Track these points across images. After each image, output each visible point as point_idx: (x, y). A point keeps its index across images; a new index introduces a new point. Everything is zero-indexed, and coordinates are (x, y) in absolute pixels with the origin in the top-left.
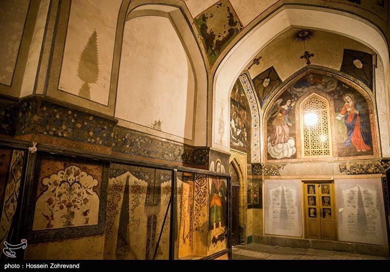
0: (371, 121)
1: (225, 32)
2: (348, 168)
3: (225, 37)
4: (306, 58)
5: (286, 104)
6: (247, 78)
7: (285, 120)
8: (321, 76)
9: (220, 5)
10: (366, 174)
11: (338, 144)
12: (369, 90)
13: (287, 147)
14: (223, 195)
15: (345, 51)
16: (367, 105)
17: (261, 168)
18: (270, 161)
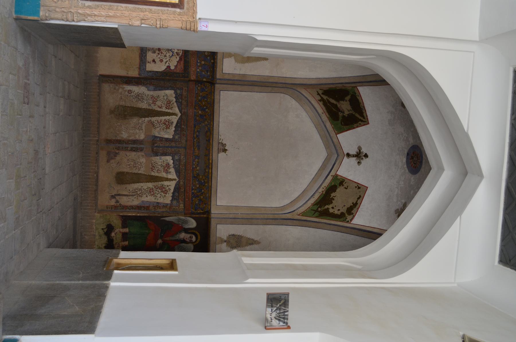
1: (339, 210)
9: (359, 188)
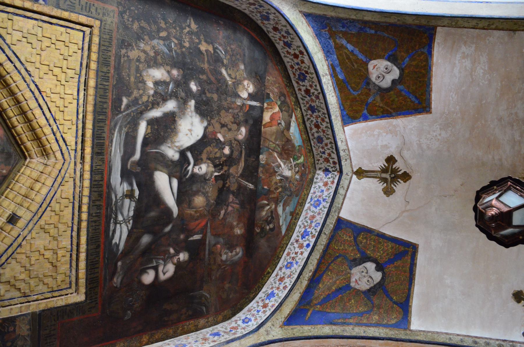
6: (332, 191)
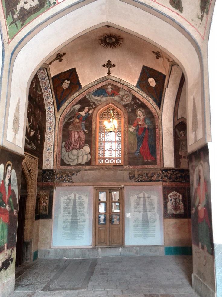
0: (157, 135)
2: (136, 176)
3: (33, 7)
4: (108, 67)
5: (84, 110)
7: (82, 126)
8: (119, 88)
10: (150, 181)
11: (129, 153)
12: (157, 108)
13: (82, 153)
14: (11, 208)
15: (143, 69)
16: (155, 121)
17: (54, 174)
18: (63, 168)
